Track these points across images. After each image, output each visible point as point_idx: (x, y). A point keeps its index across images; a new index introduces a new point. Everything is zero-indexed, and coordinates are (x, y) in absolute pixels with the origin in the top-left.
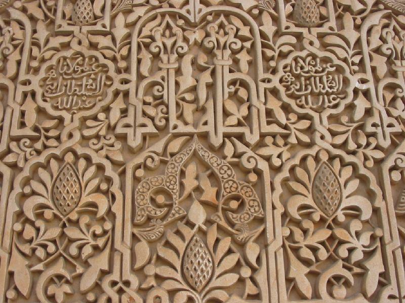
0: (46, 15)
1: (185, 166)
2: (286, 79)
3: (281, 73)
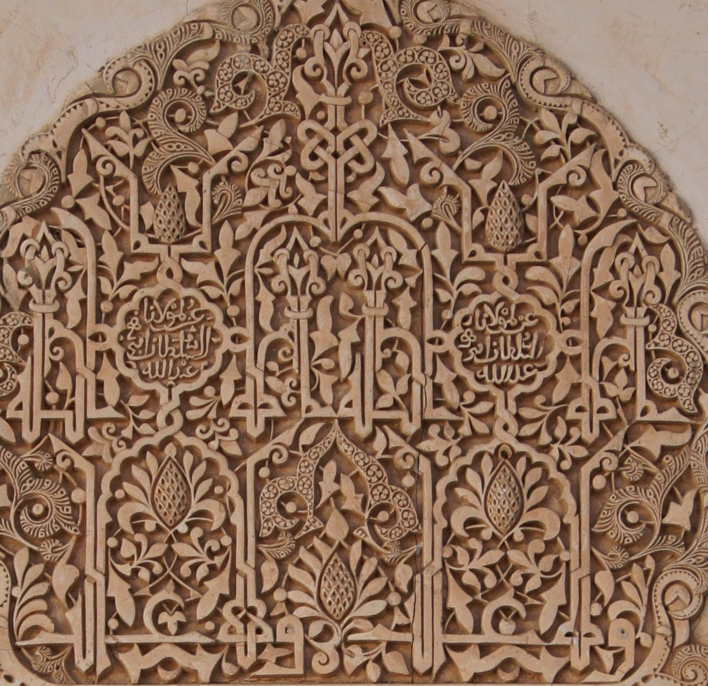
1: (323, 462)
2: (465, 338)
3: (457, 330)
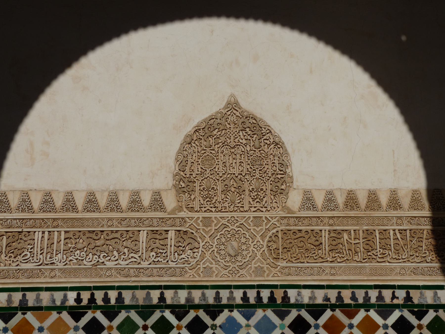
0: (200, 145)
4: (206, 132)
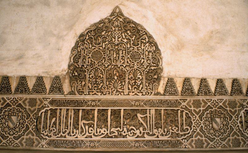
1: (114, 70)
3: (130, 55)
4: (96, 33)
